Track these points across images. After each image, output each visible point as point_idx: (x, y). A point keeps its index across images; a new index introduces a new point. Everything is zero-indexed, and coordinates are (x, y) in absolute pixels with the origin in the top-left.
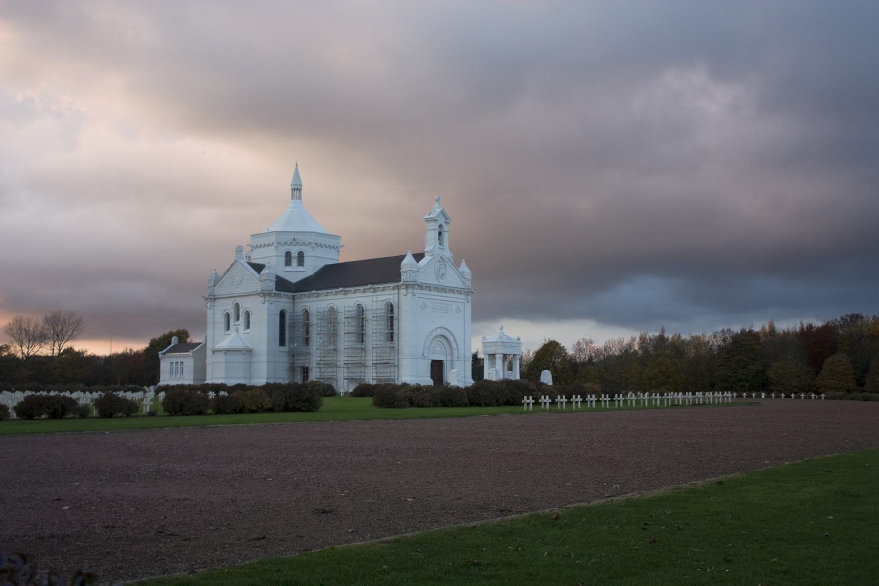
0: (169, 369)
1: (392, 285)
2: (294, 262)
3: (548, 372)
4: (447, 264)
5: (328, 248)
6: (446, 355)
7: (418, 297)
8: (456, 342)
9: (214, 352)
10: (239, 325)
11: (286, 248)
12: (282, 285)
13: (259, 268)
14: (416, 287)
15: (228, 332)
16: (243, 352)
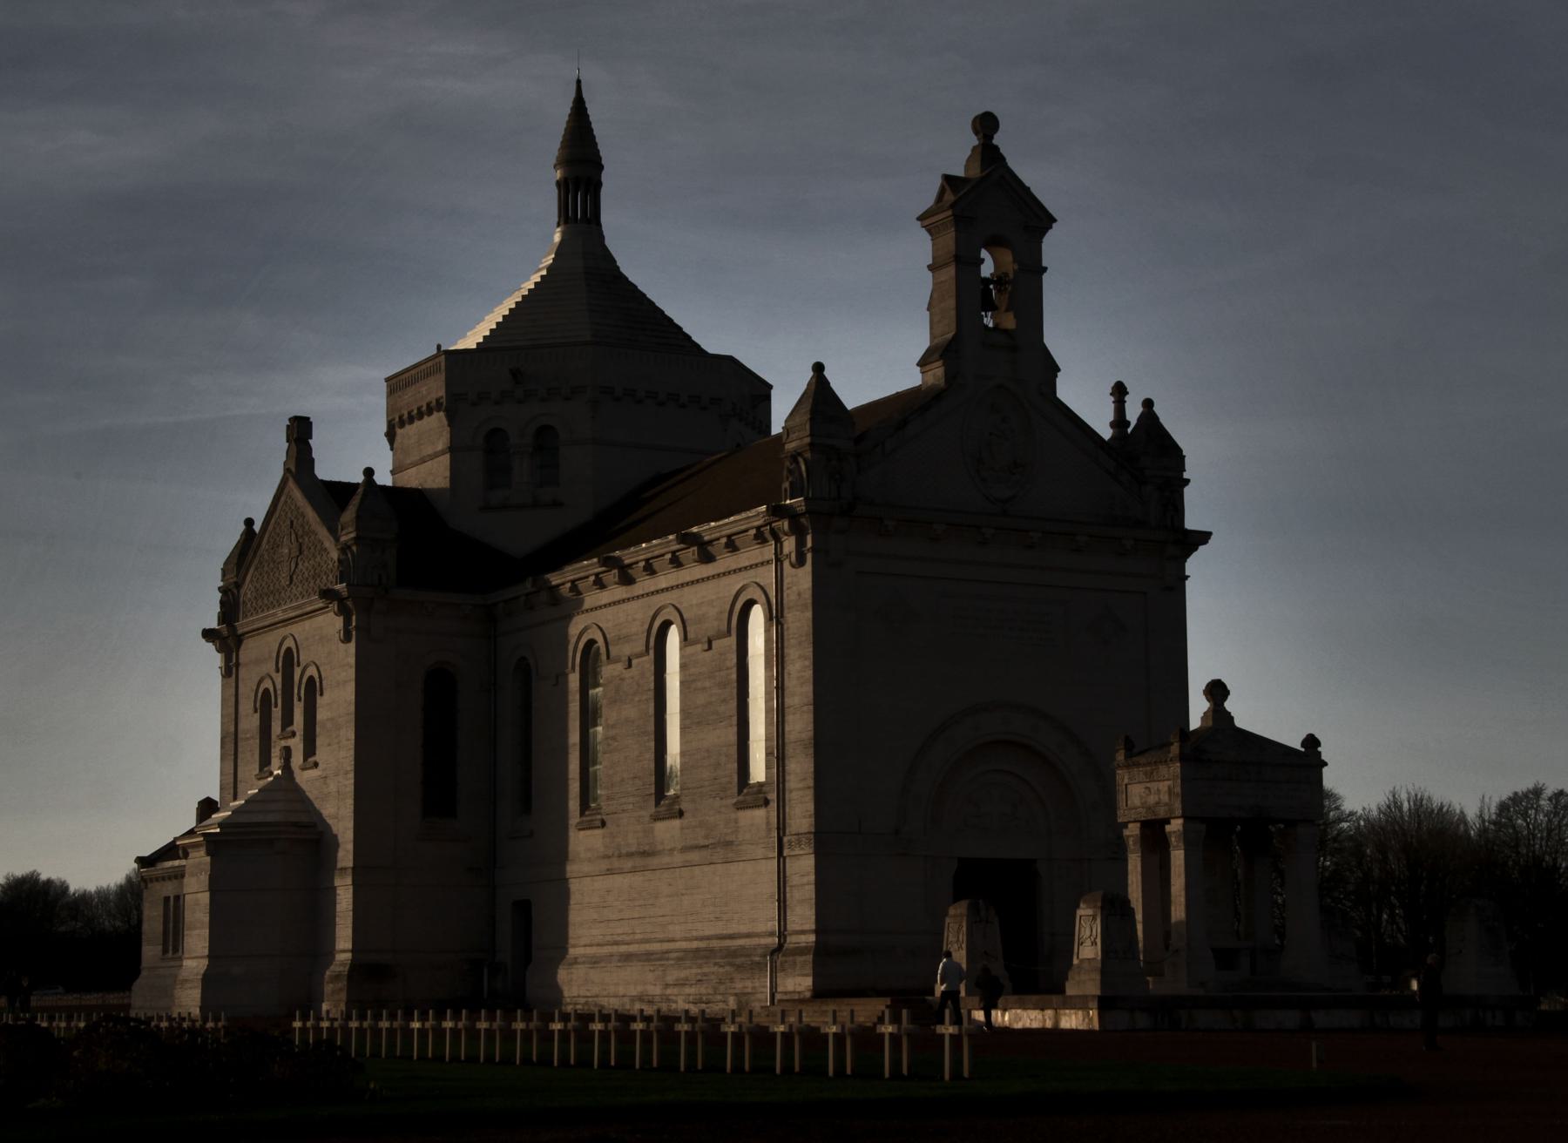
10: (294, 734)
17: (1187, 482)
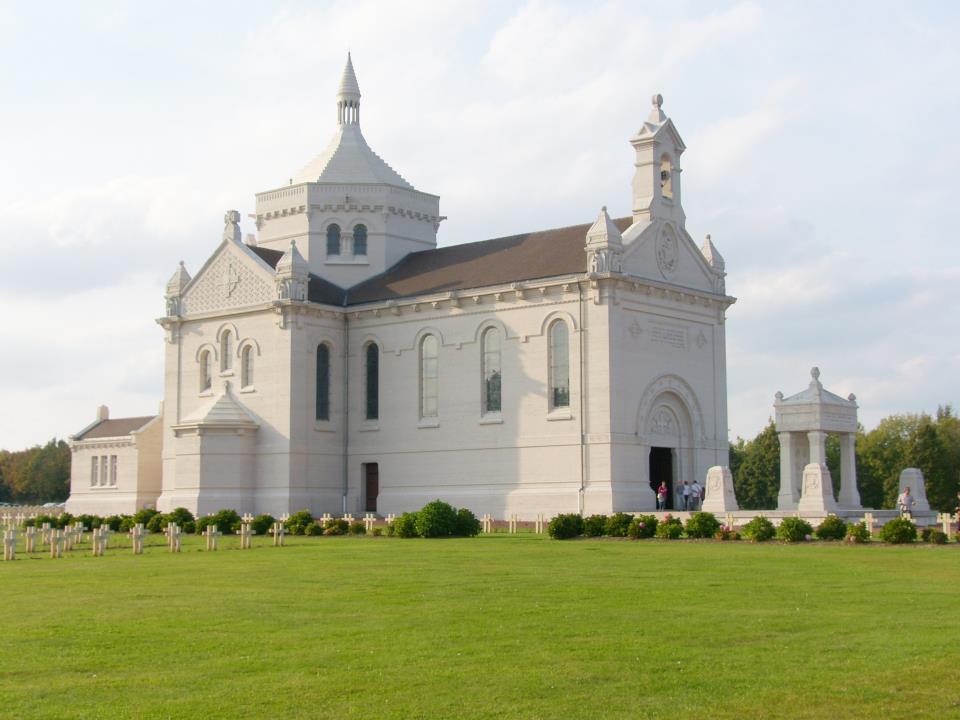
0: (88, 471)
1: (565, 281)
2: (346, 246)
3: (917, 473)
4: (679, 241)
5: (416, 219)
6: (680, 437)
7: (624, 309)
8: (699, 409)
9: (178, 433)
10: (233, 375)
11: (330, 217)
12: (321, 291)
13: (271, 257)
14: (621, 284)
15: (208, 392)
16: (241, 432)
17: (726, 274)
